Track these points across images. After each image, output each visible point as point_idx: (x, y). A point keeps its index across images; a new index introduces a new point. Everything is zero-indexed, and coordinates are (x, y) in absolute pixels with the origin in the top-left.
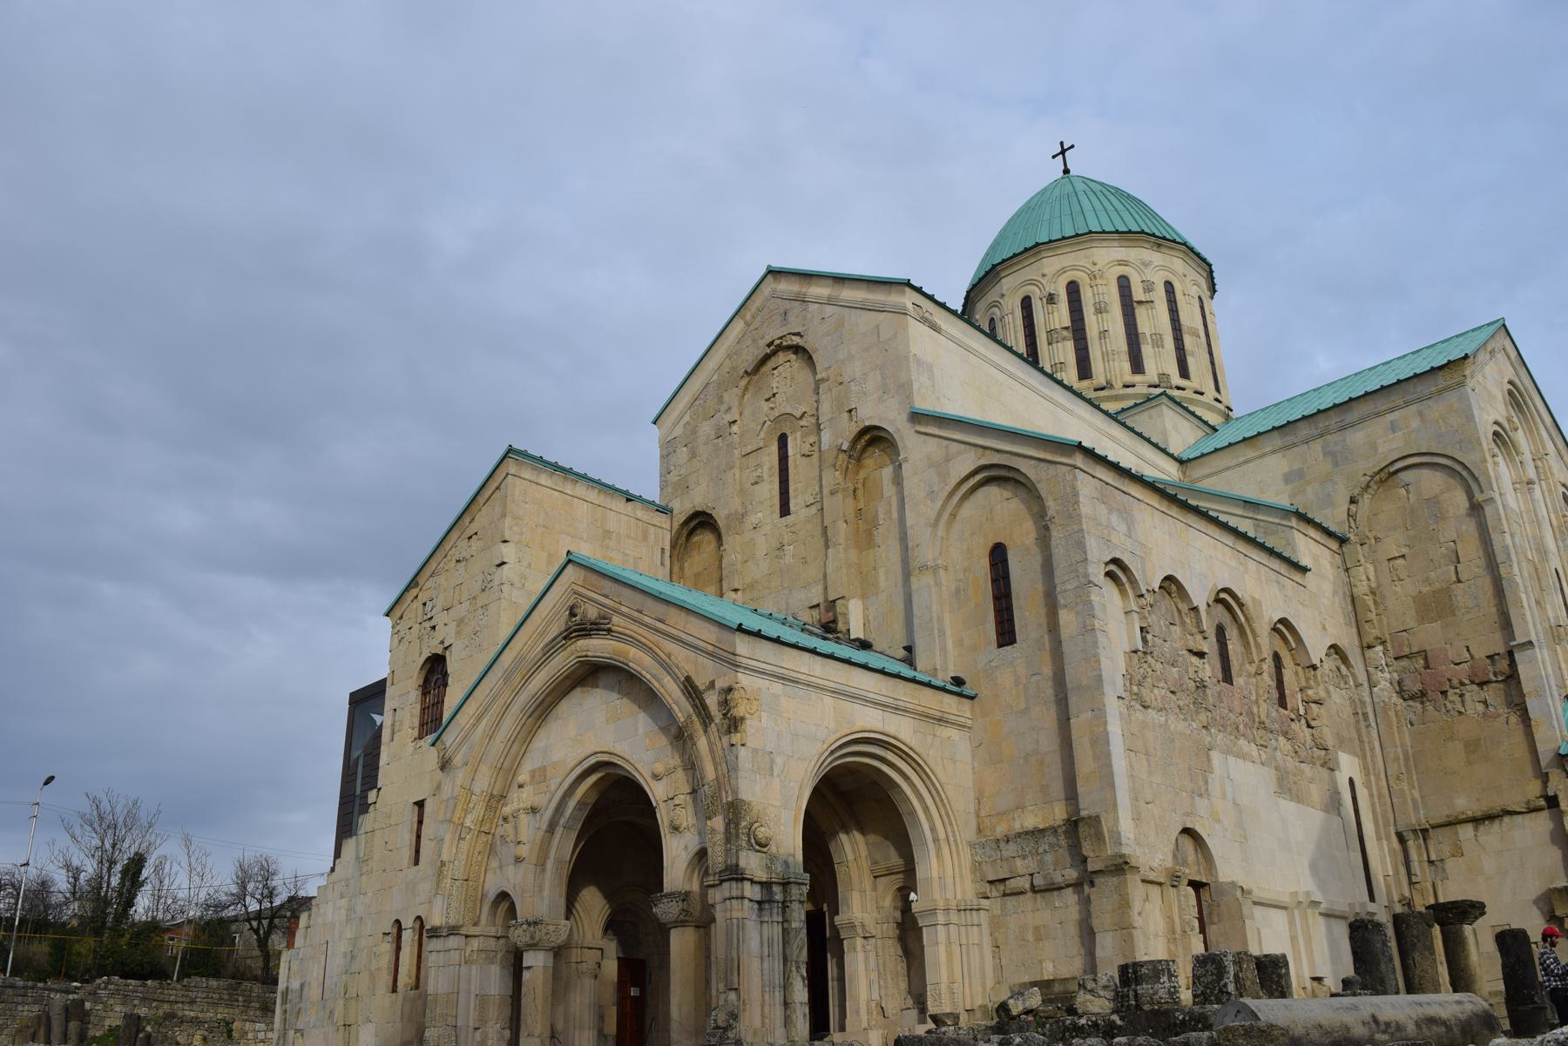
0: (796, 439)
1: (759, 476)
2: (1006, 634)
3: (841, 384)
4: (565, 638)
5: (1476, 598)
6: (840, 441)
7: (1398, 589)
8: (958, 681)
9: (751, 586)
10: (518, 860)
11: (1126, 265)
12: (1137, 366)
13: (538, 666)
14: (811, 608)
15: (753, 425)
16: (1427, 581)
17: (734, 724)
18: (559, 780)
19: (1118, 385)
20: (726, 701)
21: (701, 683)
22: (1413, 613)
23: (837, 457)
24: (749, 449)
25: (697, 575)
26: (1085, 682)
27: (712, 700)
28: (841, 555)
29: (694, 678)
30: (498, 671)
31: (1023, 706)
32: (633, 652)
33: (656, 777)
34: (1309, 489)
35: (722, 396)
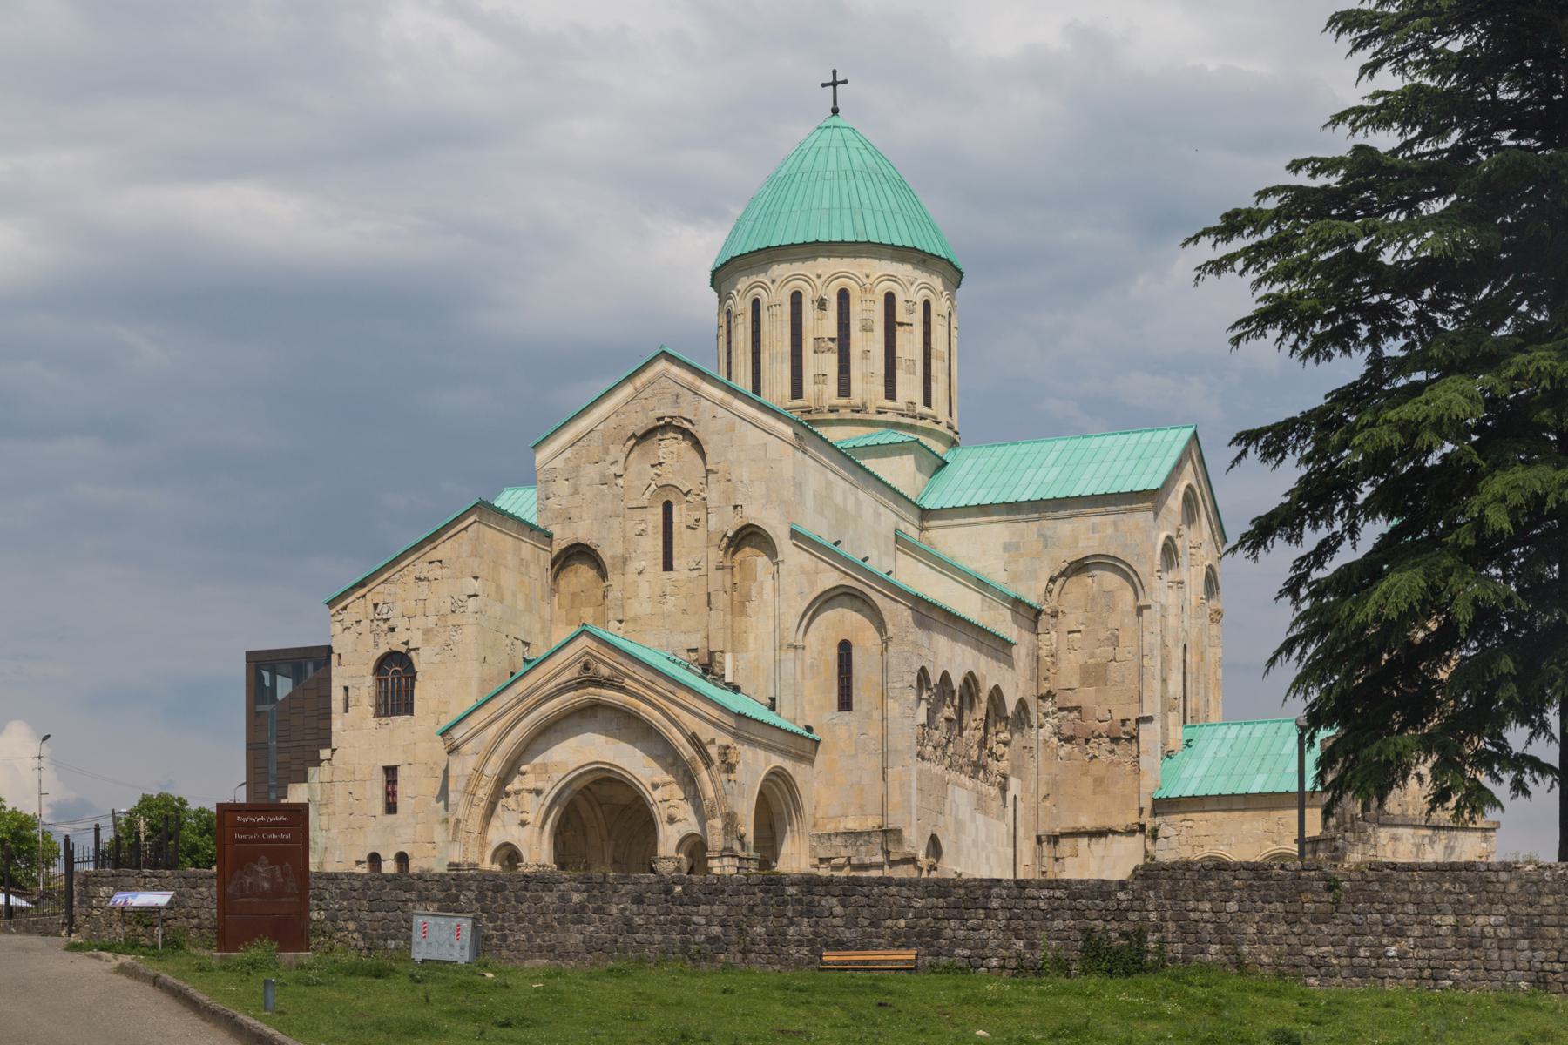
0: (681, 509)
2: (845, 703)
3: (729, 480)
4: (578, 683)
5: (1123, 676)
6: (726, 529)
8: (809, 729)
9: (635, 620)
11: (895, 281)
12: (890, 393)
14: (690, 650)
15: (638, 483)
16: (1092, 656)
17: (730, 768)
19: (872, 409)
21: (704, 738)
22: (1078, 677)
25: (574, 595)
26: (900, 748)
27: (713, 751)
28: (717, 619)
29: (698, 733)
31: (853, 752)
32: (643, 706)
33: (655, 786)
34: (1021, 560)
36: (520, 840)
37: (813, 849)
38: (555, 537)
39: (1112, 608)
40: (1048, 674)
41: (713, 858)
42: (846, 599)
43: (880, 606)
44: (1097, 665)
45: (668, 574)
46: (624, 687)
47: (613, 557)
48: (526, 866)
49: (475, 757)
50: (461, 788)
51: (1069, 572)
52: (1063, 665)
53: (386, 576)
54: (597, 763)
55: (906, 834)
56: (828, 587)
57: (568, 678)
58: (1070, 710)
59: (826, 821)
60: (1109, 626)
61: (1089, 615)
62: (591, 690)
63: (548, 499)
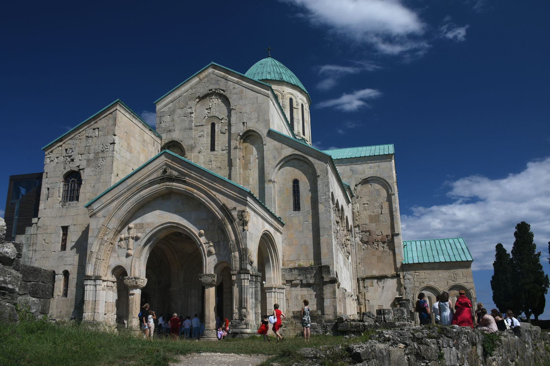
1: (202, 135)
2: (297, 207)
4: (160, 179)
7: (365, 212)
10: (128, 255)
13: (145, 187)
18: (150, 229)
20: (242, 215)
24: (198, 124)
26: (326, 226)
27: (235, 214)
29: (227, 204)
30: (124, 185)
31: (301, 230)
32: (195, 191)
35: (187, 102)
36: (126, 265)
37: (283, 276)
38: (163, 139)
39: (379, 195)
40: (357, 218)
41: (234, 274)
43: (313, 162)
44: (375, 215)
45: (212, 153)
46: (185, 181)
47: (188, 146)
48: (129, 279)
49: (104, 218)
50: (95, 235)
51: (362, 183)
52: (362, 216)
53: (72, 136)
54: (170, 223)
55: (331, 269)
57: (155, 177)
58: (366, 232)
59: (289, 262)
60: (379, 202)
61: (371, 198)
62: (167, 183)
63: (161, 123)
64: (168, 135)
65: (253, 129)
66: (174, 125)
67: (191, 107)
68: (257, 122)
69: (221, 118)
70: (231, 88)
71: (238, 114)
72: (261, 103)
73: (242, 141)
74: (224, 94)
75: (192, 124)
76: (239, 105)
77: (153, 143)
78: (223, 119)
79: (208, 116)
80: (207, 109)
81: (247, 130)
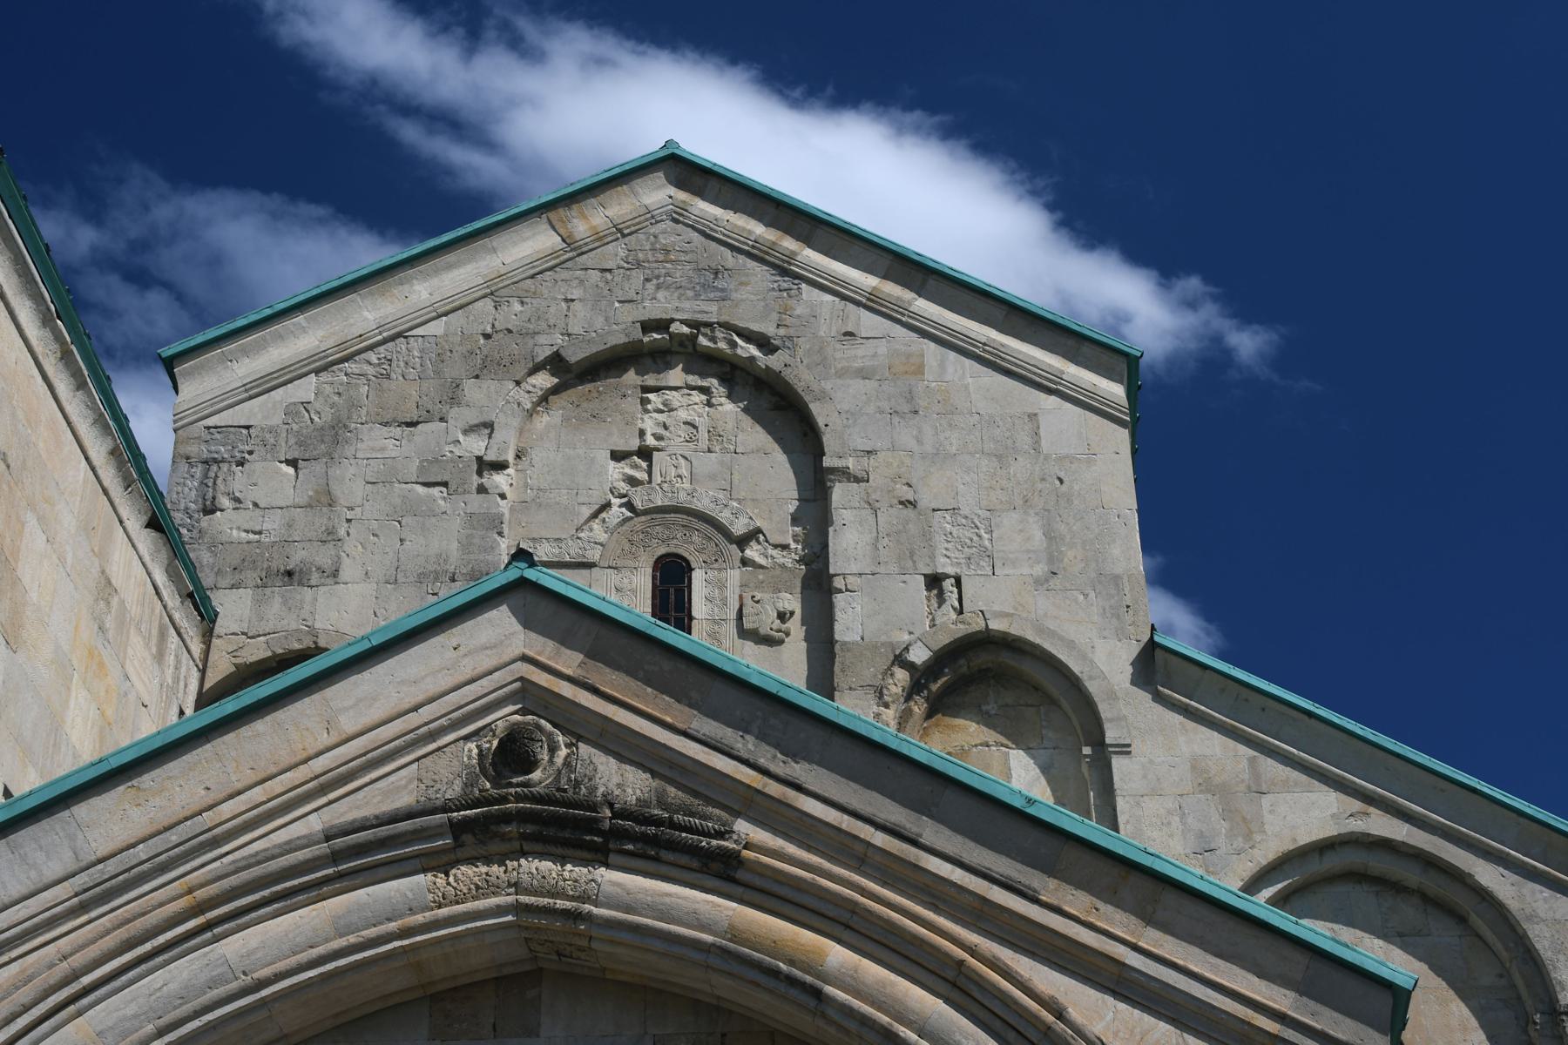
23: (888, 672)
42: (1361, 896)
56: (1305, 838)
64: (278, 600)
65: (1015, 630)
66: (331, 532)
67: (489, 426)
68: (1039, 582)
69: (739, 528)
70: (827, 328)
71: (890, 516)
72: (1071, 459)
73: (919, 707)
74: (774, 362)
75: (493, 548)
76: (893, 448)
77: (155, 632)
78: (754, 535)
79: (629, 506)
80: (617, 456)
81: (961, 630)
